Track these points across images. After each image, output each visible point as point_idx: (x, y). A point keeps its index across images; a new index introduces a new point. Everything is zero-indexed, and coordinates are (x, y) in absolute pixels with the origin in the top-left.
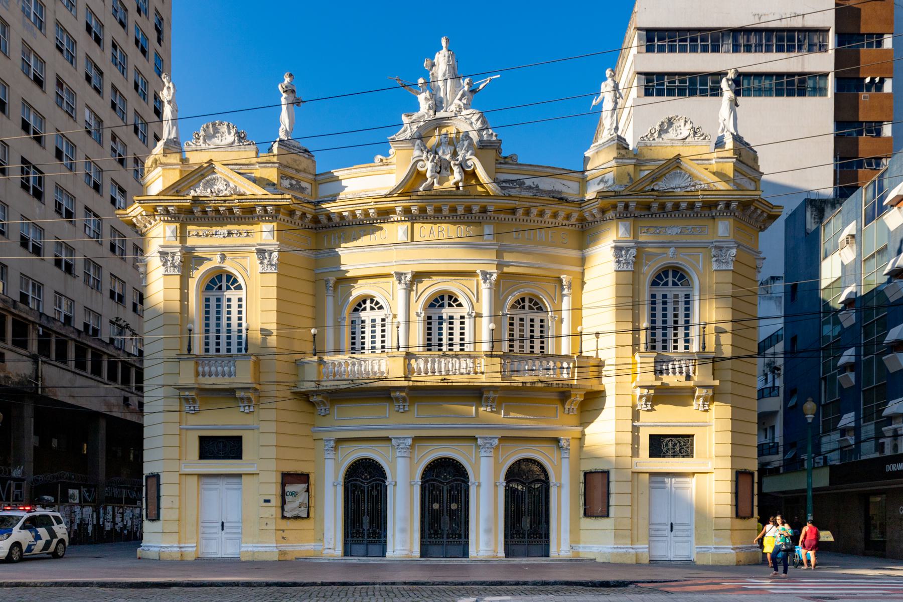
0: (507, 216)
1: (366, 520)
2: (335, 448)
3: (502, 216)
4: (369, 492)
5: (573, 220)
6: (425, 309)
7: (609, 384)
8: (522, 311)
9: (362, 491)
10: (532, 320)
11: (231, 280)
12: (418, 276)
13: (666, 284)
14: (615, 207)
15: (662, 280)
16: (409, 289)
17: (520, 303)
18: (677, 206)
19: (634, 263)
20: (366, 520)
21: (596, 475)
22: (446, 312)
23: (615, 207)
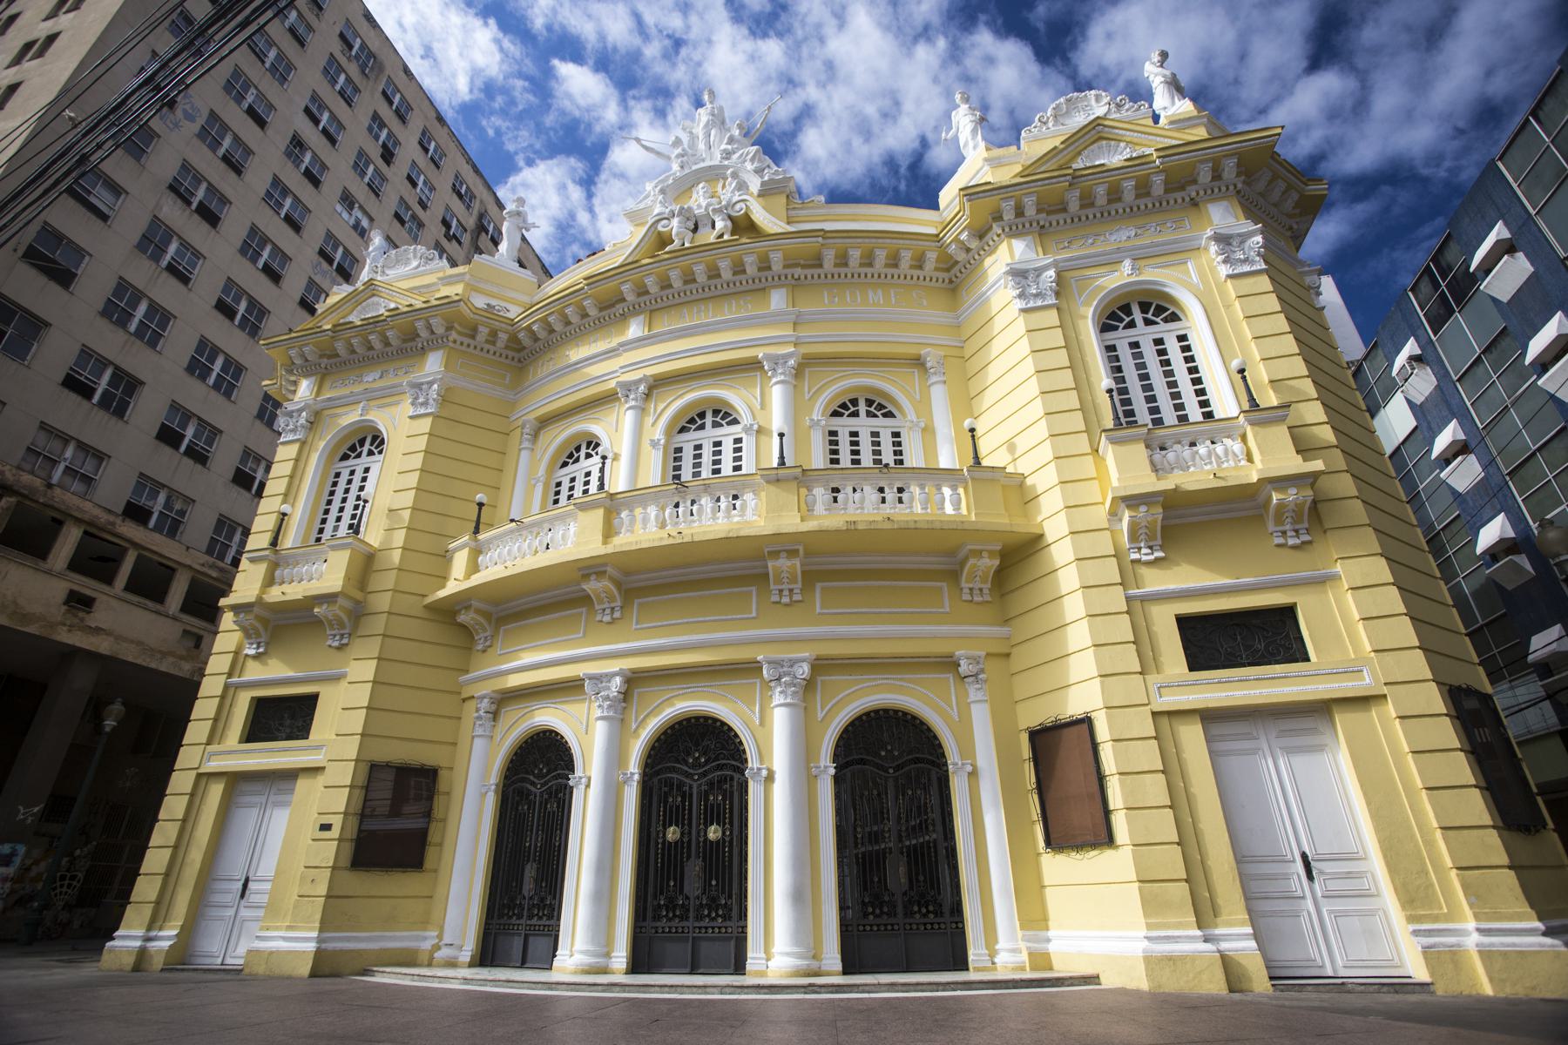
0: (809, 272)
1: (530, 872)
2: (495, 715)
3: (798, 271)
4: (543, 804)
5: (930, 265)
6: (668, 433)
7: (1052, 520)
8: (853, 420)
9: (531, 804)
10: (875, 434)
11: (378, 441)
12: (658, 385)
13: (1132, 325)
14: (998, 217)
15: (1121, 320)
16: (642, 411)
17: (845, 408)
18: (1115, 195)
19: (1057, 294)
20: (530, 872)
21: (1066, 731)
22: (708, 436)
23: (998, 217)
